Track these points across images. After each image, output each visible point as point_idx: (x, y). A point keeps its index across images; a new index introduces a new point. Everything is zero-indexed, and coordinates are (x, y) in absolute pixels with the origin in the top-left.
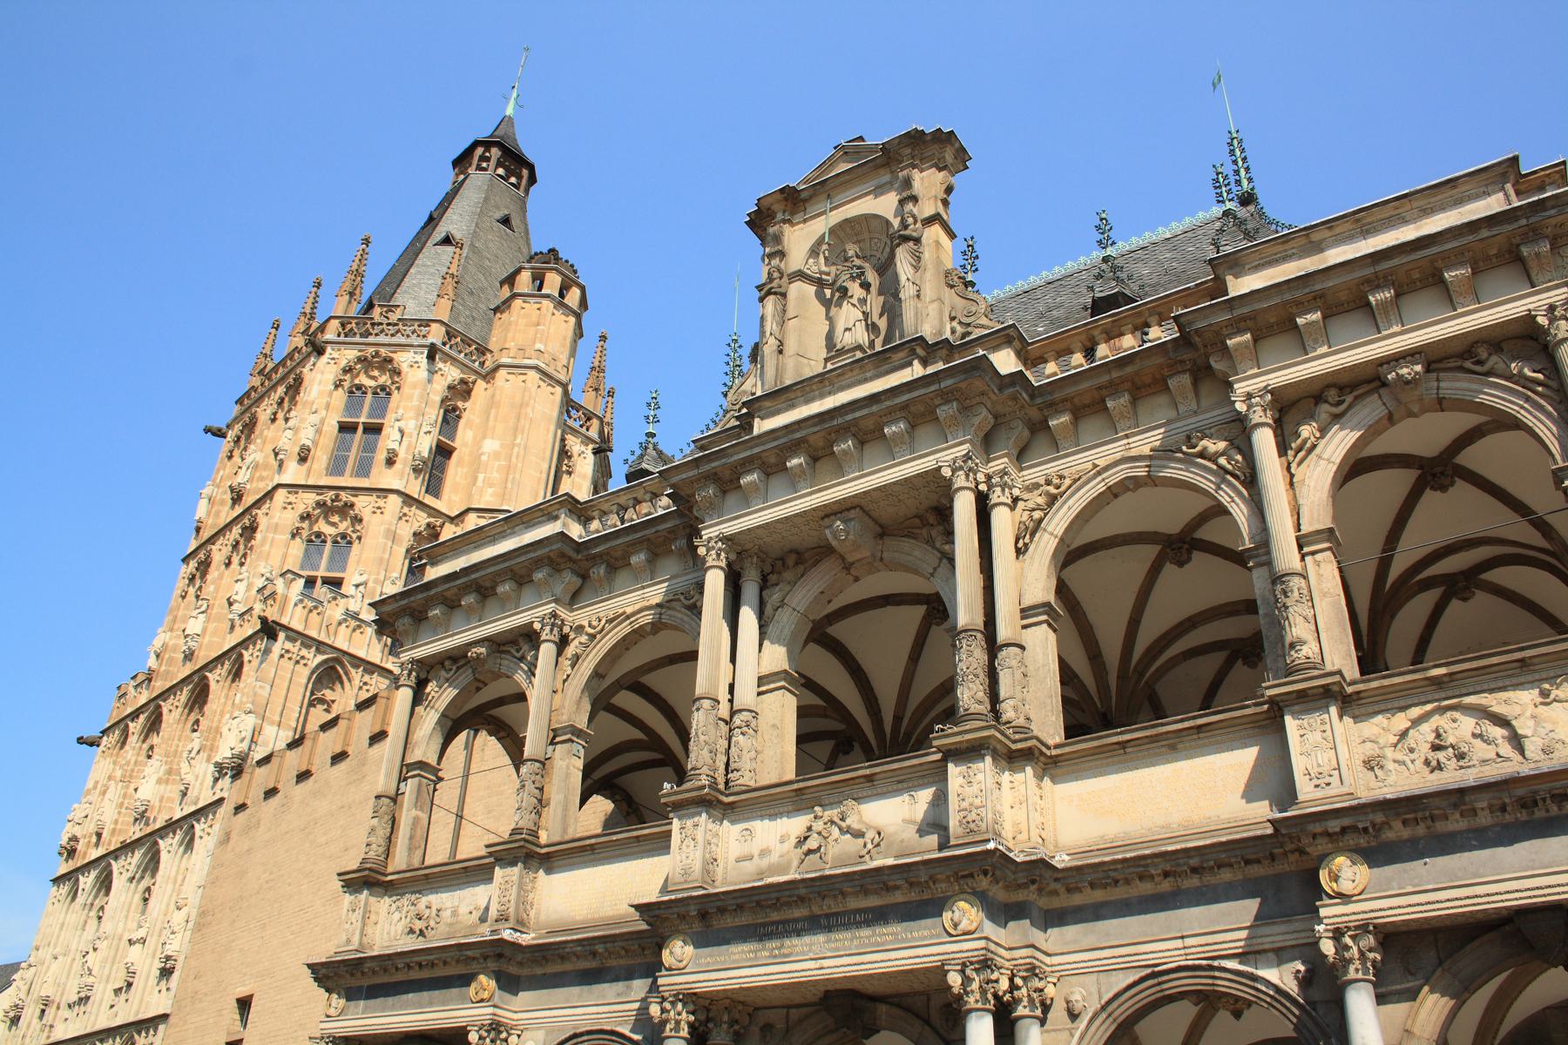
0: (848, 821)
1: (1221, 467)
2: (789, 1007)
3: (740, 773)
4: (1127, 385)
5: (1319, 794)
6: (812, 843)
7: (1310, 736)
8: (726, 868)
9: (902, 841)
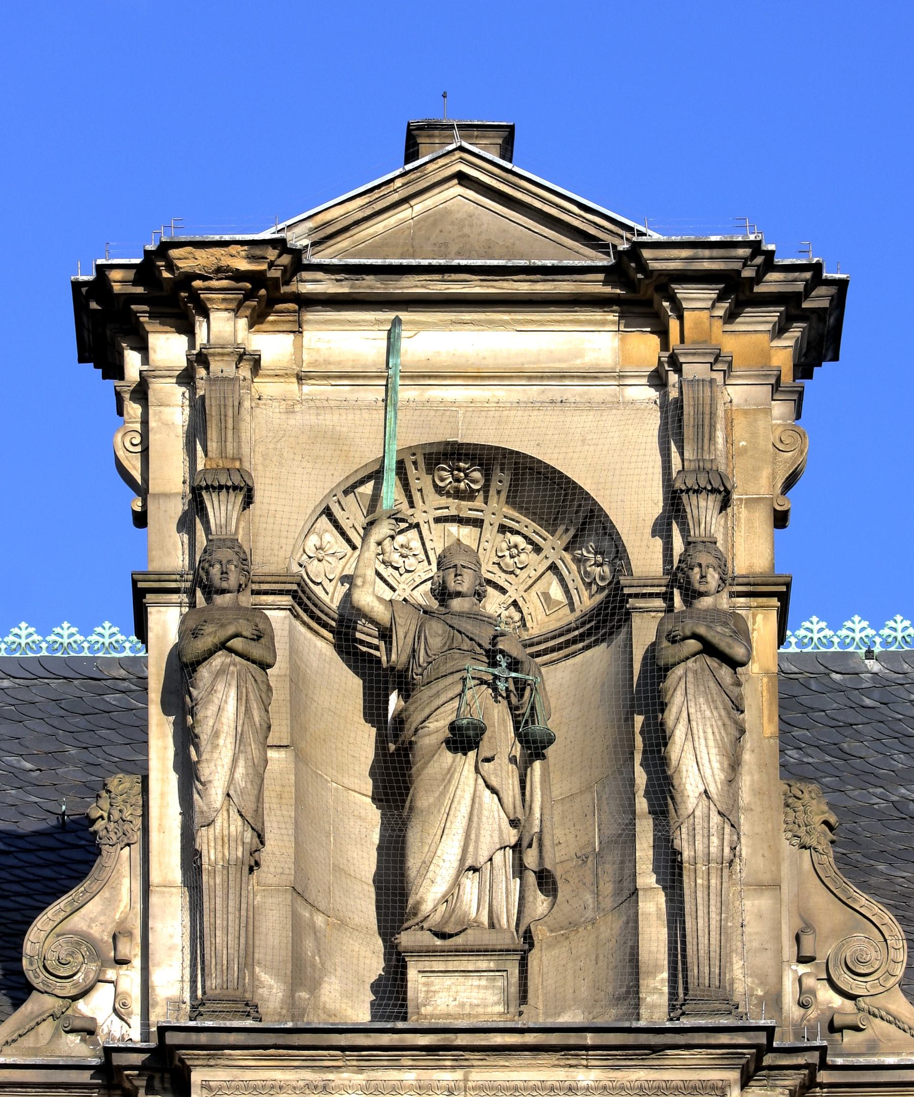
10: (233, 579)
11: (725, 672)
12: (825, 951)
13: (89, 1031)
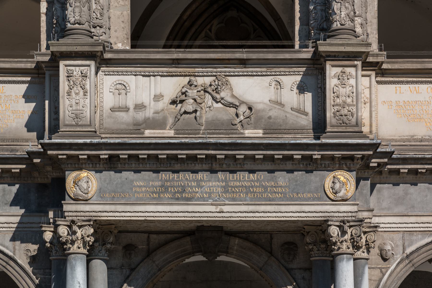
0: (223, 94)
2: (150, 233)
3: (102, 30)
6: (189, 106)
8: (101, 115)
9: (270, 118)
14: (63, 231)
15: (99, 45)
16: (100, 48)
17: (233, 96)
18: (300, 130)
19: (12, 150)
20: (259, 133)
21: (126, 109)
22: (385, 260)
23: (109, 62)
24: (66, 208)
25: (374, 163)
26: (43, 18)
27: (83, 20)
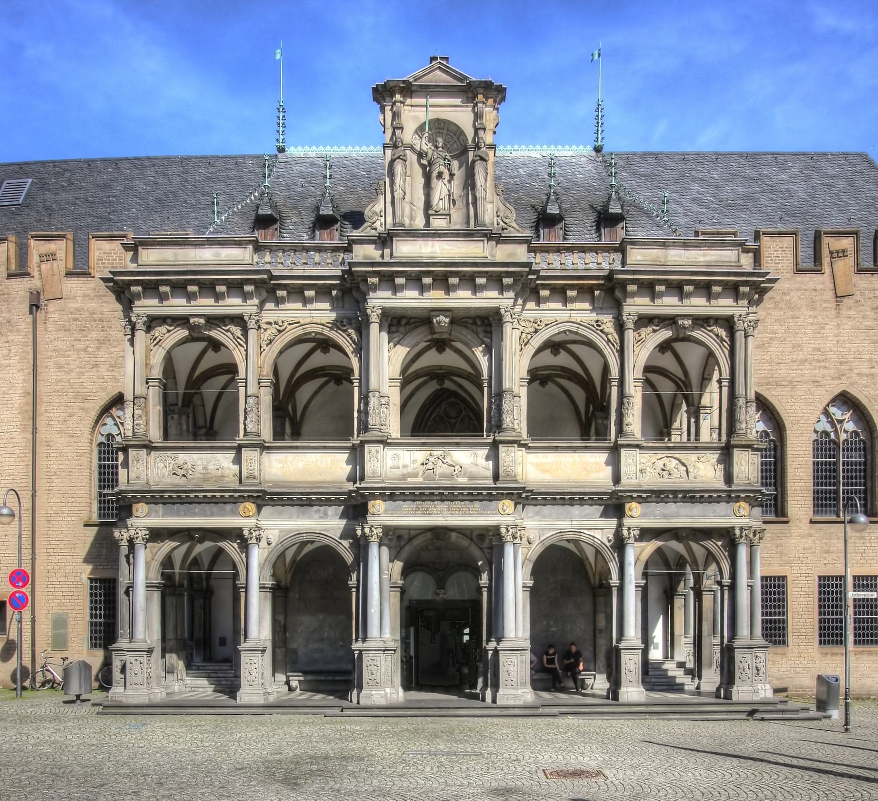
1: (609, 340)
4: (577, 287)
5: (628, 481)
7: (628, 460)
10: (400, 144)
11: (484, 163)
12: (502, 215)
13: (376, 229)
14: (367, 530)
15: (385, 436)
16: (386, 438)
17: (453, 461)
18: (484, 478)
19: (340, 488)
20: (466, 479)
21: (399, 468)
22: (530, 543)
23: (389, 444)
24: (368, 519)
25: (524, 495)
26: (356, 420)
27: (377, 423)
